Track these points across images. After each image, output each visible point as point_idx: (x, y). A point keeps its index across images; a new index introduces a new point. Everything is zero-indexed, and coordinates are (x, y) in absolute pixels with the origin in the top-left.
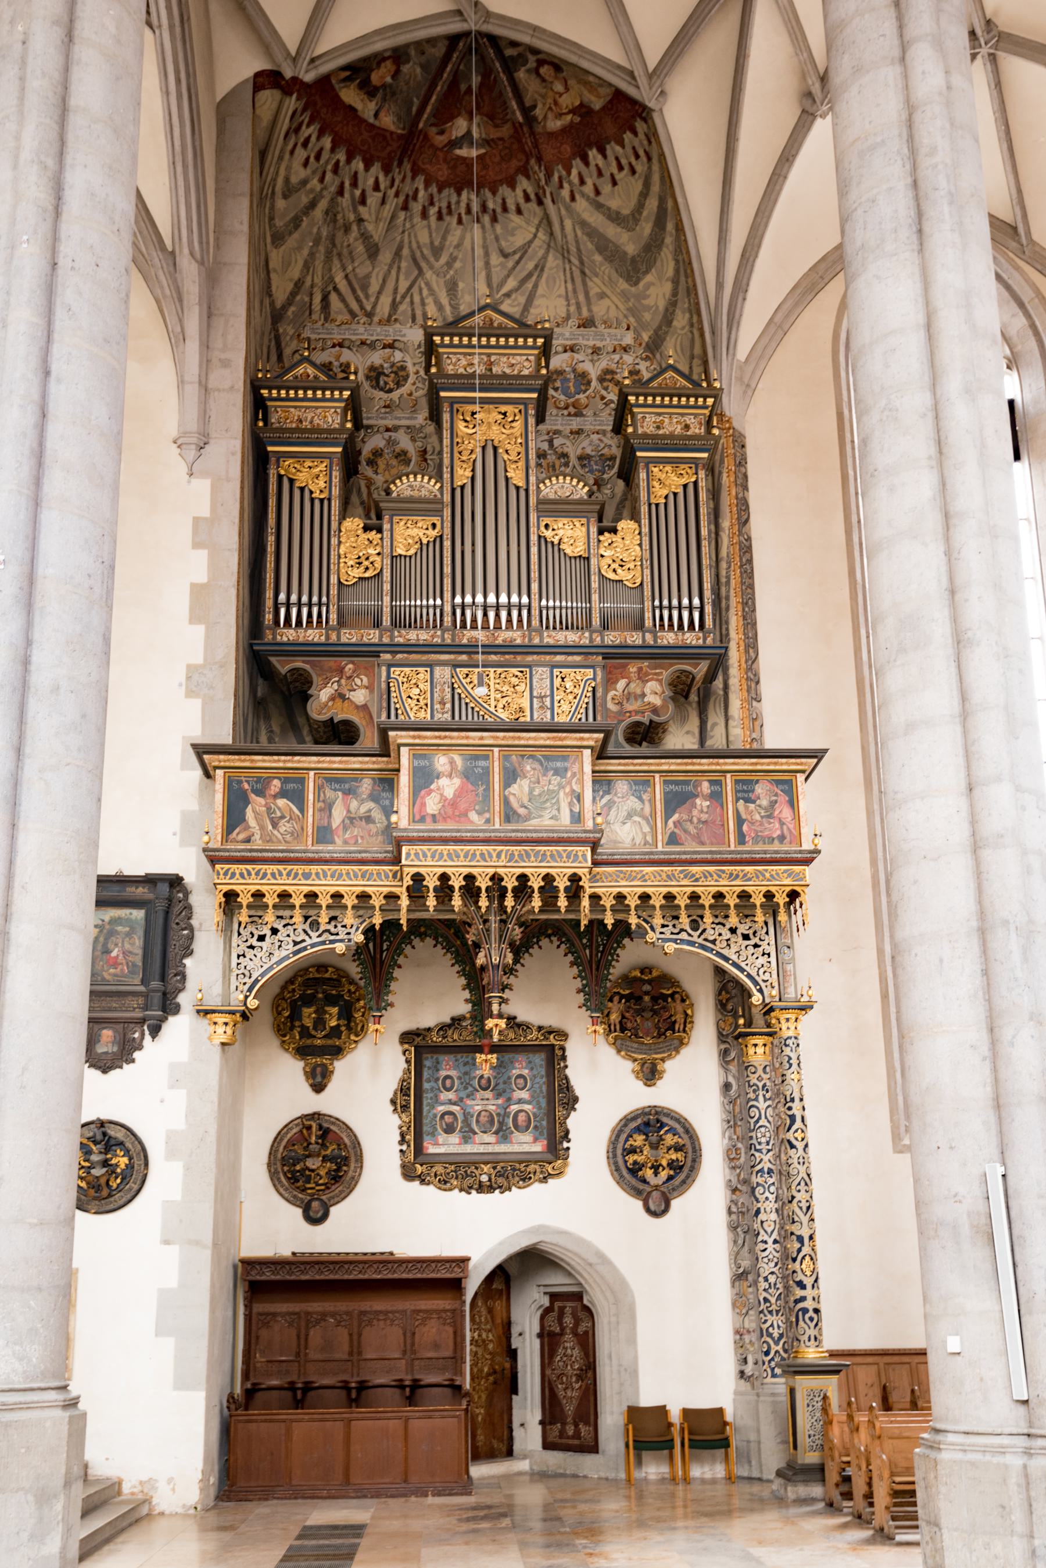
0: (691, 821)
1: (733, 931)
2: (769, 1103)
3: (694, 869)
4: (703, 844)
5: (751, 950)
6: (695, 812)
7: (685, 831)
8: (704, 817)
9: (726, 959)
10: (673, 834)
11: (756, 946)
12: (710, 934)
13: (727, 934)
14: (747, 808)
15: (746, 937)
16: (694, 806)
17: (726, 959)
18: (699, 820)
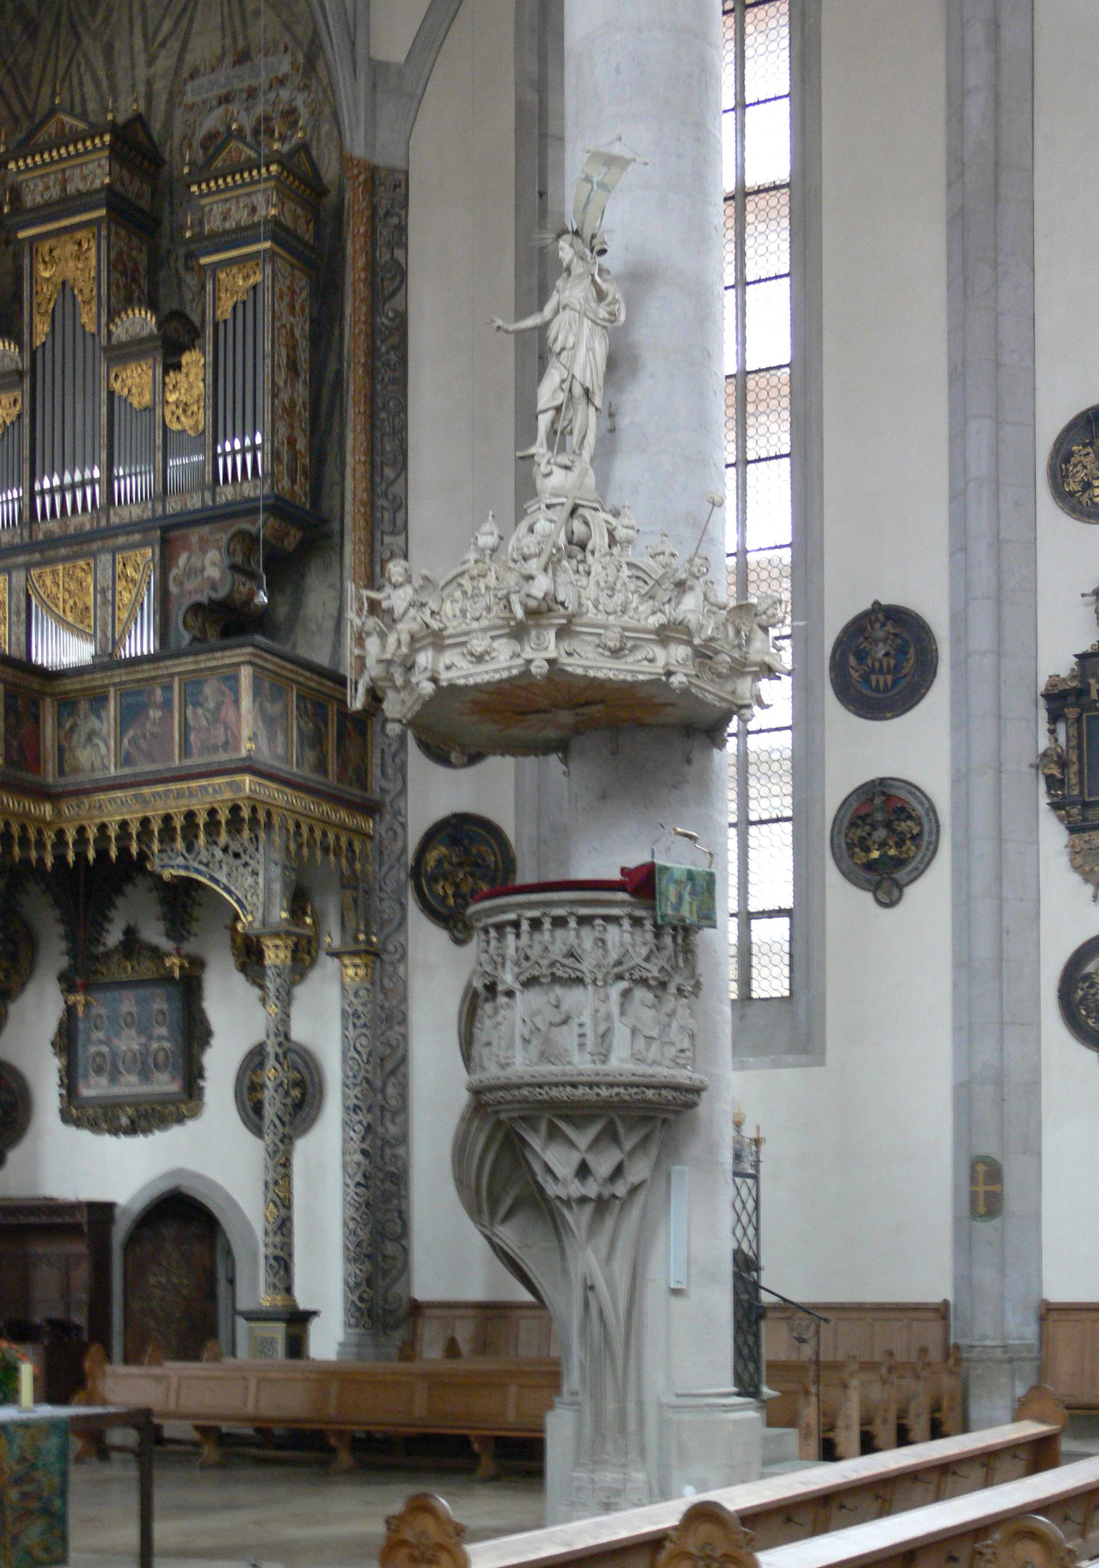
0: (144, 737)
1: (225, 850)
2: (359, 1031)
3: (146, 790)
4: (153, 760)
5: (241, 869)
6: (149, 726)
7: (138, 748)
8: (156, 730)
9: (217, 882)
10: (128, 754)
11: (246, 864)
12: (204, 856)
13: (219, 854)
14: (195, 714)
15: (237, 855)
16: (147, 717)
17: (217, 882)
18: (152, 734)
